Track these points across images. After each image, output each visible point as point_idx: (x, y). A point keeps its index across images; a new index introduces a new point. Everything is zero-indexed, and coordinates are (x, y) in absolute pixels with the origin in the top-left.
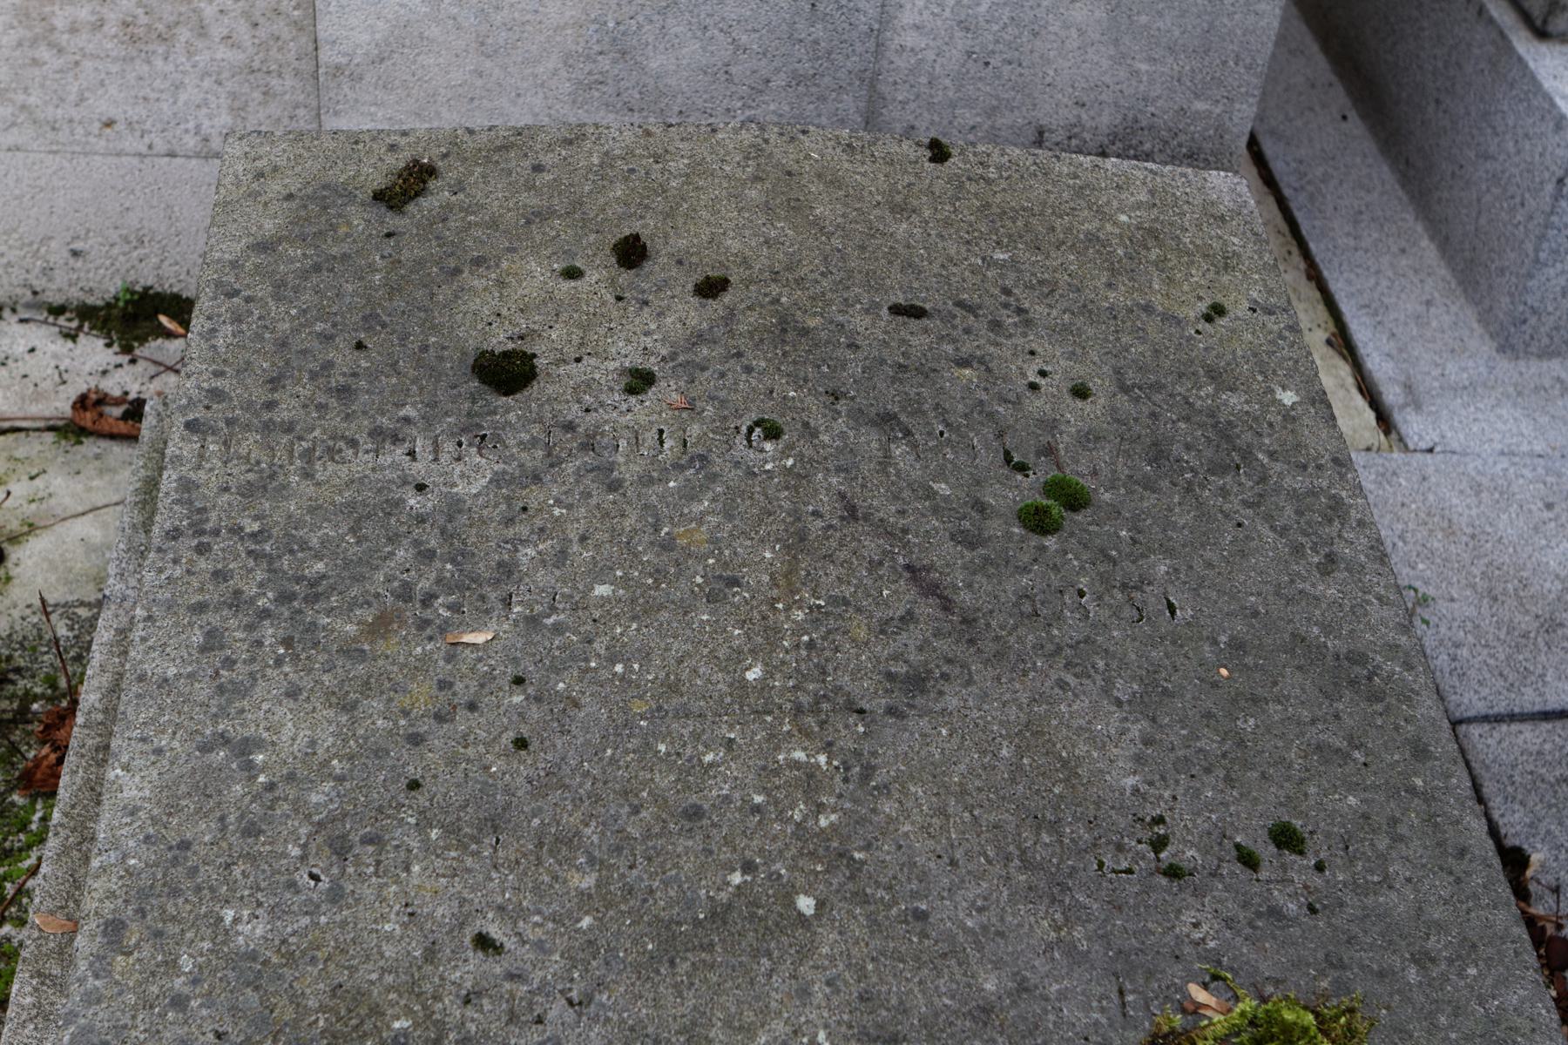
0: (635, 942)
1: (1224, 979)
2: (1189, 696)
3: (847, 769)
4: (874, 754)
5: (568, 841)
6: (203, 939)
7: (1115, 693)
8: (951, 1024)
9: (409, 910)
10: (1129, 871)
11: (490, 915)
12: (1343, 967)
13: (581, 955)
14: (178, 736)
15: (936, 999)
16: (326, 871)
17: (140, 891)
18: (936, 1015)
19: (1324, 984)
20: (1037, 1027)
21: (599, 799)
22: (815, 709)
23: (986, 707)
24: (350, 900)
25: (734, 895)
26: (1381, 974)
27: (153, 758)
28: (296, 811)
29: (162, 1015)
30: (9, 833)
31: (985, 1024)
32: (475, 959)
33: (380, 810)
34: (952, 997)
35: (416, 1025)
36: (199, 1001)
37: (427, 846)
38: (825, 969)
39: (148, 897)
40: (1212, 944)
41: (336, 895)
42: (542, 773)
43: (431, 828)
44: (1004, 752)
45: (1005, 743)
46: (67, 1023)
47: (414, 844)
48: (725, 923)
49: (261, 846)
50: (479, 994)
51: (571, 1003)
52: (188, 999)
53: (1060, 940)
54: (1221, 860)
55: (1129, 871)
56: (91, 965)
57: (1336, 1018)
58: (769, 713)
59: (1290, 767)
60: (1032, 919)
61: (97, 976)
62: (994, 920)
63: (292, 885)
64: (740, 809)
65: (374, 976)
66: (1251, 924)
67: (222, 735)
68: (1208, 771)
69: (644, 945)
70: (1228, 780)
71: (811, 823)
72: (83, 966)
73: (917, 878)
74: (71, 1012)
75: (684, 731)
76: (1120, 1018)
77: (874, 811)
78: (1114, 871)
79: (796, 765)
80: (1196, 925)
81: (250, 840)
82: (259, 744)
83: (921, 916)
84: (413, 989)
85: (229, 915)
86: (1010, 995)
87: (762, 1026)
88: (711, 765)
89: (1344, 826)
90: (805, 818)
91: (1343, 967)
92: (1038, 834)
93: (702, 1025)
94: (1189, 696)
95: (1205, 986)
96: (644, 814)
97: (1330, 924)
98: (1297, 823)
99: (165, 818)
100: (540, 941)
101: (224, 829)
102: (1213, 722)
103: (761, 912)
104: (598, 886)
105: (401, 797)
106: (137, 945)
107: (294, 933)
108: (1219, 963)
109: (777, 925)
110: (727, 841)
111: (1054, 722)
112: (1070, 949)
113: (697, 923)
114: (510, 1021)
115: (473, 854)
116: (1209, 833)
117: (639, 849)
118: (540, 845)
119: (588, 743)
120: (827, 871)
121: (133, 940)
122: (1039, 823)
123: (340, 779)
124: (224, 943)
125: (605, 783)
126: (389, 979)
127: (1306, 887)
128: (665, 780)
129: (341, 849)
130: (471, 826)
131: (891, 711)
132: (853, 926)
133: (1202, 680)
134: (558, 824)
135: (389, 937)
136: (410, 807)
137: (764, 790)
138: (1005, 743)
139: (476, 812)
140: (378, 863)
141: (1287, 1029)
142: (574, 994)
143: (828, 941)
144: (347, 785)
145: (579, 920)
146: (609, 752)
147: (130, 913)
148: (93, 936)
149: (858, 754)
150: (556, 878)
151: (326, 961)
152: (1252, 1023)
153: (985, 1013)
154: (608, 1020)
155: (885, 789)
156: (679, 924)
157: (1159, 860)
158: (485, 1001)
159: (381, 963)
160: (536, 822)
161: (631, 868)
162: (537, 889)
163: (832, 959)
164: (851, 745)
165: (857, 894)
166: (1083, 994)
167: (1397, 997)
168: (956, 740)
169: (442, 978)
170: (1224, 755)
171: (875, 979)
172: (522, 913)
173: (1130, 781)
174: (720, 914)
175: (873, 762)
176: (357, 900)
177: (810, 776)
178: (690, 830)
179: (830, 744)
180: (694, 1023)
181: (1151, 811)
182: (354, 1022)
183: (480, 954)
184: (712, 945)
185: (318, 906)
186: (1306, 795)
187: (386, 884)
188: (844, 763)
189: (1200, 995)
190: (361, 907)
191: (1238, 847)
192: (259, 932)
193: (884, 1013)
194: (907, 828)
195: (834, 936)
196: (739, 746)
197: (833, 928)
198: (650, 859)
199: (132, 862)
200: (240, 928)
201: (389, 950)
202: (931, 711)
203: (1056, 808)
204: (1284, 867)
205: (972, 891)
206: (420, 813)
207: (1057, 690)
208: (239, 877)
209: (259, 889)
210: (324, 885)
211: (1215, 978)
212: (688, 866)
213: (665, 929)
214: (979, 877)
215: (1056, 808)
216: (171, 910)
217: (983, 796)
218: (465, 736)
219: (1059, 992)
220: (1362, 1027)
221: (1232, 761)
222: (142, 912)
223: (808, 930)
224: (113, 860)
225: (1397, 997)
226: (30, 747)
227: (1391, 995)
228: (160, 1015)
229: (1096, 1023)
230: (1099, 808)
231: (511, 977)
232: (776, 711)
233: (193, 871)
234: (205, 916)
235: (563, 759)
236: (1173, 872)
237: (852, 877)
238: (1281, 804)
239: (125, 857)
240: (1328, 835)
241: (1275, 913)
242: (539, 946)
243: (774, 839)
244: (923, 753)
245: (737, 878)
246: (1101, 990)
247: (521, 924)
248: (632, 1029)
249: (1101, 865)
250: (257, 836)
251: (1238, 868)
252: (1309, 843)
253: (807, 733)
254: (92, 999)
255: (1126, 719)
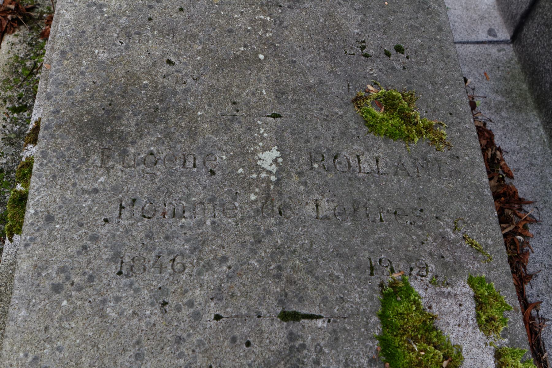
0: (212, 64)
1: (378, 84)
2: (375, 9)
3: (275, 21)
4: (283, 18)
5: (194, 37)
6: (89, 57)
7: (354, 7)
8: (300, 90)
9: (148, 52)
10: (354, 54)
11: (171, 55)
12: (411, 83)
13: (197, 67)
14: (81, 2)
15: (296, 84)
16: (125, 41)
17: (71, 44)
18: (296, 88)
19: (405, 87)
20: (324, 93)
21: (203, 26)
22: (267, 5)
23: (317, 8)
24: (131, 49)
25: (241, 53)
26: (421, 86)
27: (74, 8)
28: (116, 24)
29: (78, 76)
30: (38, 50)
31: (310, 91)
32: (167, 66)
33: (140, 25)
34: (301, 83)
35: (150, 83)
36: (88, 73)
37: (154, 36)
38: (266, 74)
39: (73, 45)
40: (375, 75)
41: (127, 48)
42: (187, 18)
43: (155, 31)
44: (321, 20)
45: (321, 18)
46: (51, 77)
47: (150, 35)
48: (238, 60)
49: (106, 33)
50: (168, 75)
51: (194, 79)
52: (85, 72)
53: (332, 71)
54: (380, 53)
55: (354, 54)
56: (57, 62)
57: (407, 96)
58: (254, 5)
59: (402, 30)
60: (325, 65)
61: (59, 65)
62: (314, 64)
63: (115, 44)
64: (244, 31)
65: (138, 69)
66: (387, 71)
67: (94, 3)
68: (379, 30)
69: (215, 65)
70: (384, 32)
71: (264, 35)
72: (55, 63)
73: (293, 52)
74: (52, 74)
75: (229, 9)
76: (347, 92)
77: (282, 33)
78: (349, 54)
79: (261, 19)
80: (371, 70)
81: (103, 31)
82: (105, 6)
83: (294, 62)
84: (149, 73)
85: (96, 51)
86: (317, 84)
87: (247, 88)
88: (236, 18)
89: (416, 47)
90: (262, 34)
91: (411, 83)
92: (329, 43)
93: (230, 87)
94: (375, 9)
95: (372, 86)
96: (216, 30)
97: (409, 72)
98: (403, 45)
99: (78, 24)
100: (185, 62)
101: (95, 28)
102: (382, 17)
103: (248, 58)
104: (202, 49)
105: (146, 22)
106: (70, 58)
107: (115, 57)
108: (377, 80)
109: (253, 62)
110: (240, 39)
111: (336, 13)
112: (335, 74)
113: (230, 60)
114: (176, 83)
115: (167, 39)
116: (377, 46)
117: (214, 40)
118: (186, 37)
119: (200, 10)
120: (268, 48)
121: (69, 57)
122: (329, 40)
123: (129, 16)
124: (95, 58)
125: (205, 21)
126: (142, 70)
127: (403, 62)
128: (223, 22)
129: (129, 35)
130: (166, 31)
131: (289, 7)
132: (274, 63)
133: (380, 5)
134: (191, 32)
135: (142, 59)
136: (149, 25)
137: (251, 26)
138: (321, 18)
139: (168, 27)
140: (139, 40)
141: (394, 97)
142: (195, 77)
143: (267, 66)
144: (131, 18)
145: (196, 58)
146: (207, 13)
147: (68, 49)
148: (57, 55)
149: (279, 18)
150: (190, 46)
151: (124, 65)
152: (384, 96)
153: (310, 88)
154: (204, 84)
155: (286, 28)
156: (225, 60)
157: (362, 52)
158: (169, 77)
159: (140, 66)
160: (185, 31)
161: (212, 44)
162: (185, 49)
163: (268, 71)
164: (277, 15)
165: (276, 55)
166: (338, 85)
167: (425, 92)
168: (307, 16)
169: (157, 71)
170: (384, 26)
171: (279, 77)
172: (181, 55)
173: (356, 31)
174: (237, 58)
175: (283, 20)
176: (133, 49)
177: (265, 23)
178: (229, 35)
179: (271, 14)
180: (228, 86)
181: (361, 39)
182: (132, 81)
183: (168, 65)
184: (234, 66)
185: (122, 50)
186: (406, 38)
187: (142, 45)
188: (274, 20)
189: (370, 88)
190: (134, 51)
191: (385, 50)
192: (105, 56)
193: (282, 86)
194: (291, 38)
195: (269, 65)
196: (245, 14)
197: (269, 63)
198: (217, 43)
199: (68, 36)
200: (100, 55)
201: (142, 63)
202: (301, 8)
203: (335, 36)
204: (398, 57)
205: (309, 56)
206: (152, 27)
207: (337, 5)
208: (99, 41)
209: (105, 45)
210: (124, 44)
211: (375, 84)
212: (228, 45)
213: (221, 62)
214: (311, 53)
215: (335, 36)
216: (80, 49)
217: (314, 32)
218: (165, 7)
219: (331, 84)
220: (414, 99)
221: (386, 28)
222: (71, 49)
223: (262, 63)
224: (63, 35)
225: (425, 92)
226: (43, 26)
227: (424, 92)
228: (77, 76)
229: (341, 93)
230: (347, 37)
231: (177, 71)
232: (256, 5)
233: (86, 39)
234: (90, 51)
235: (193, 14)
236: (366, 56)
237: (275, 50)
238: (399, 40)
239: (66, 34)
240: (411, 49)
241: (394, 68)
242: (185, 63)
243: (253, 39)
244: (297, 19)
245: (242, 49)
246: (343, 84)
247: (180, 58)
248: (211, 86)
249: (346, 52)
250: (104, 31)
251: (384, 56)
252: (405, 51)
253: (265, 11)
254: (58, 71)
255: (357, 14)
